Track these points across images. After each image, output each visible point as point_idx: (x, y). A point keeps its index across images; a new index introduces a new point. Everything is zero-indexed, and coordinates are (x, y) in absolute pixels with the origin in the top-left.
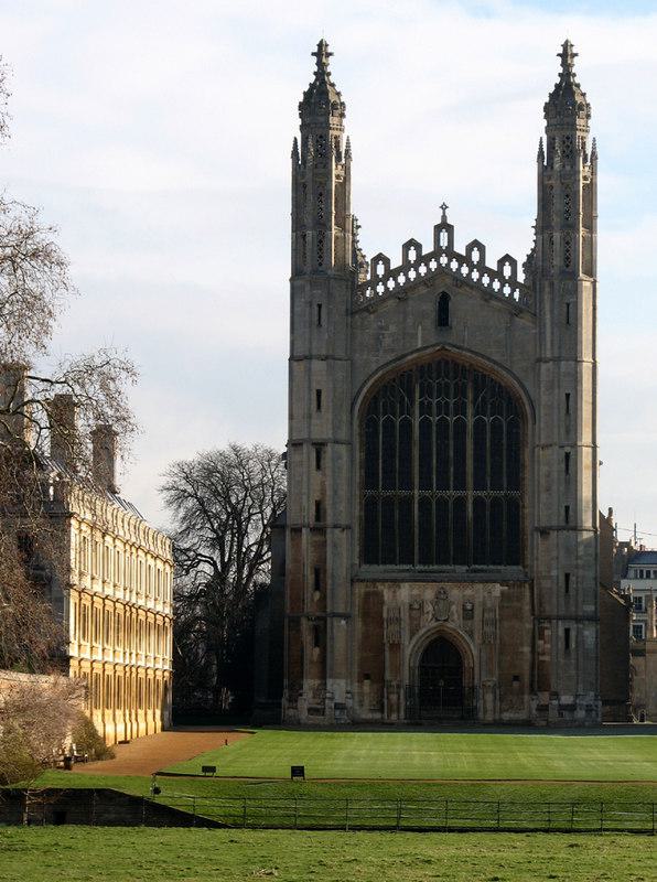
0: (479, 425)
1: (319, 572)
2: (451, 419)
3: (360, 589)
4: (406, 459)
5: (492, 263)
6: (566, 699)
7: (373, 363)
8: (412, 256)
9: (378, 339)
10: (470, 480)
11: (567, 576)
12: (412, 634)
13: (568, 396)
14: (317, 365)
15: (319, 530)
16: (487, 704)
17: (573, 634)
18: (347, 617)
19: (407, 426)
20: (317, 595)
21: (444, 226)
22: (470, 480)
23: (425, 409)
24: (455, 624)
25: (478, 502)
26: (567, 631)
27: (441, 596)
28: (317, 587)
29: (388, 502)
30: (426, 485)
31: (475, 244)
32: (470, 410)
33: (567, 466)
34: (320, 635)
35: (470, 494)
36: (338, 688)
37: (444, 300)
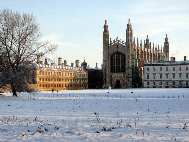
6: (128, 86)
7: (111, 52)
9: (111, 50)
14: (105, 53)
15: (105, 69)
16: (122, 86)
19: (115, 59)
21: (117, 38)
23: (116, 57)
24: (119, 78)
25: (121, 66)
29: (113, 66)
30: (116, 65)
31: (120, 40)
37: (118, 45)
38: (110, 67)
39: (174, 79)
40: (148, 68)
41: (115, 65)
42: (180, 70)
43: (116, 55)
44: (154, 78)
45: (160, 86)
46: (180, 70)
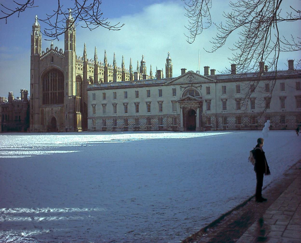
0: (59, 79)
1: (32, 106)
2: (55, 79)
3: (41, 109)
4: (49, 86)
5: (59, 51)
6: (66, 127)
8: (48, 51)
10: (57, 89)
11: (67, 105)
12: (48, 116)
13: (67, 72)
17: (67, 115)
18: (38, 114)
19: (48, 80)
20: (32, 110)
22: (57, 89)
23: (51, 77)
24: (54, 115)
25: (59, 93)
26: (66, 115)
27: (52, 109)
28: (32, 109)
31: (56, 48)
32: (57, 76)
33: (67, 85)
34: (32, 116)
35: (57, 92)
36: (36, 126)
37: (53, 57)
38: (41, 95)
39: (138, 114)
40: (94, 95)
41: (49, 91)
42: (149, 96)
43: (51, 74)
44: (104, 112)
45: (114, 128)
46: (149, 96)
